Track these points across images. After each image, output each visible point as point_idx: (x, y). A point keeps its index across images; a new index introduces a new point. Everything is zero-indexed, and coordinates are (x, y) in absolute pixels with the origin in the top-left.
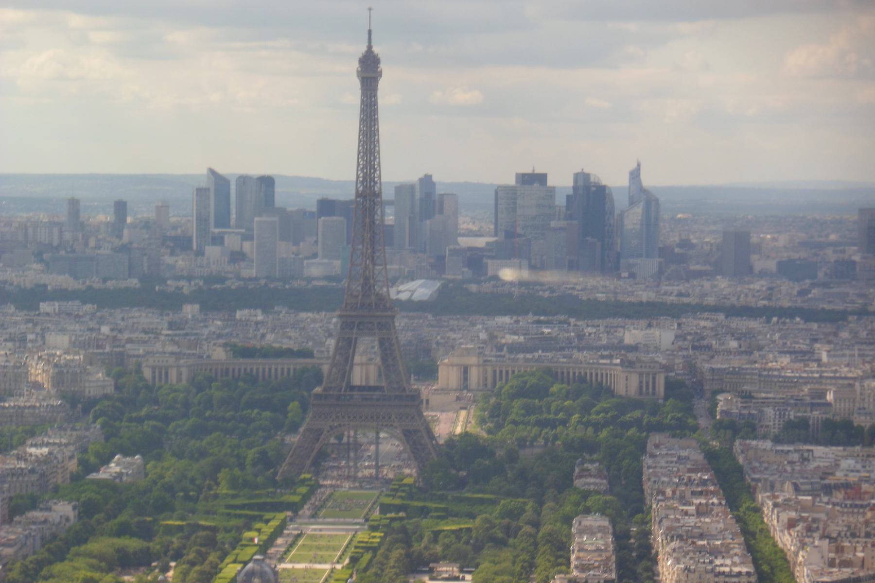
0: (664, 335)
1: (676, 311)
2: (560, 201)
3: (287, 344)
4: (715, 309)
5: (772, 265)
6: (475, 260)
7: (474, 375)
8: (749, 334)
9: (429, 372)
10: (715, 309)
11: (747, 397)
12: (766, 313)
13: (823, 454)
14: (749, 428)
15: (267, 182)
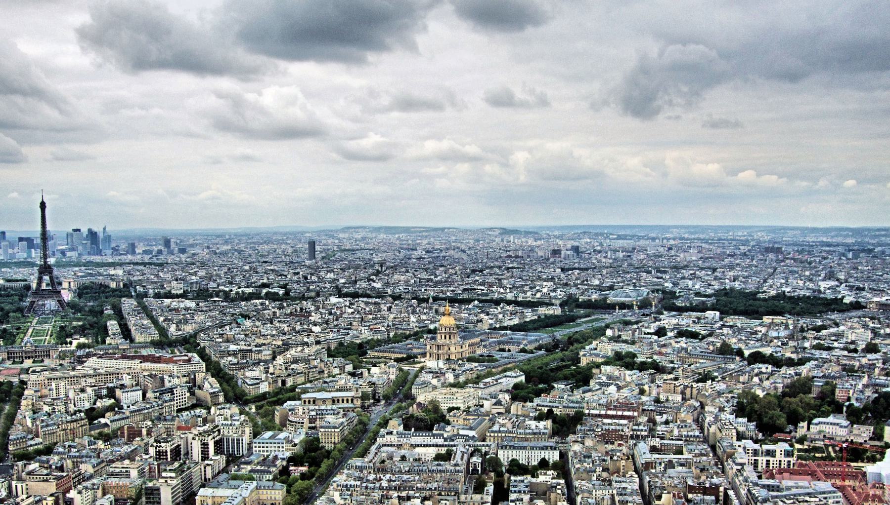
0: (119, 272)
1: (121, 265)
2: (85, 235)
3: (19, 278)
4: (129, 263)
5: (141, 251)
6: (63, 253)
7: (72, 284)
8: (142, 270)
9: (60, 284)
10: (129, 263)
11: (144, 287)
12: (144, 264)
13: (167, 301)
14: (146, 295)
15: (4, 233)
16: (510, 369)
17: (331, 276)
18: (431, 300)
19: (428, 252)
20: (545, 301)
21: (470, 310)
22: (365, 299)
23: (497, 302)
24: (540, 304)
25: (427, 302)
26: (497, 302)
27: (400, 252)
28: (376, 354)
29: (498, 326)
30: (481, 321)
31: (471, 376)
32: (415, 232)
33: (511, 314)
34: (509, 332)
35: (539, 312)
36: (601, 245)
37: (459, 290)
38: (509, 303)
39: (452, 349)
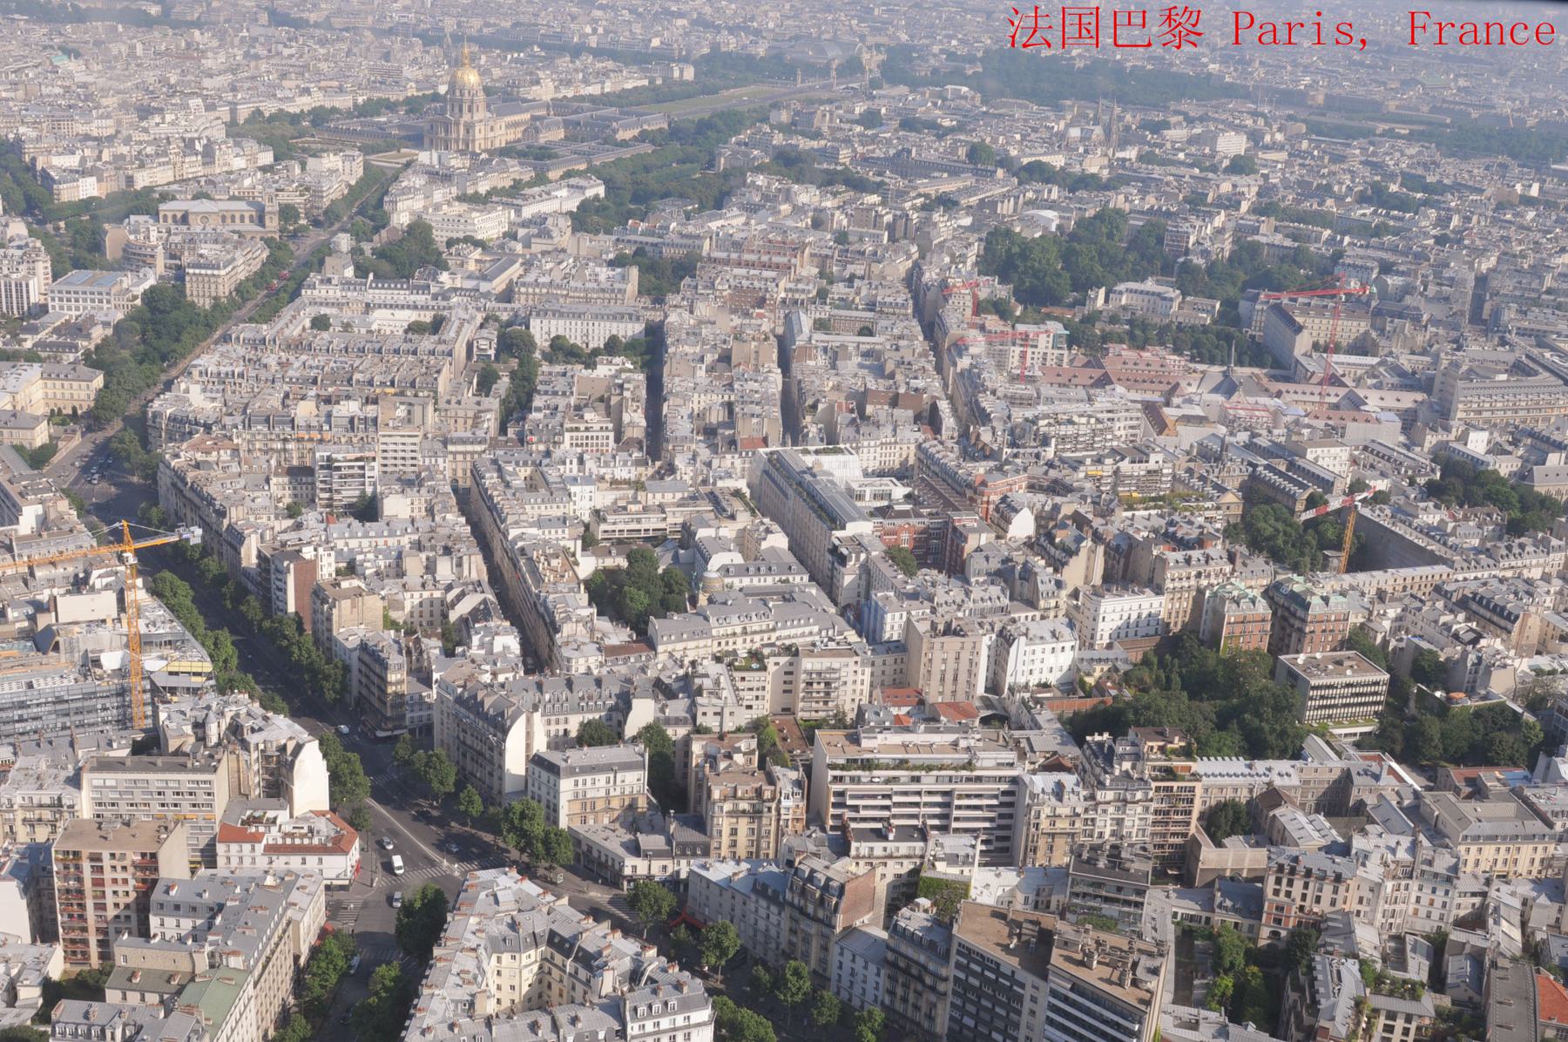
16: (579, 174)
31: (508, 183)
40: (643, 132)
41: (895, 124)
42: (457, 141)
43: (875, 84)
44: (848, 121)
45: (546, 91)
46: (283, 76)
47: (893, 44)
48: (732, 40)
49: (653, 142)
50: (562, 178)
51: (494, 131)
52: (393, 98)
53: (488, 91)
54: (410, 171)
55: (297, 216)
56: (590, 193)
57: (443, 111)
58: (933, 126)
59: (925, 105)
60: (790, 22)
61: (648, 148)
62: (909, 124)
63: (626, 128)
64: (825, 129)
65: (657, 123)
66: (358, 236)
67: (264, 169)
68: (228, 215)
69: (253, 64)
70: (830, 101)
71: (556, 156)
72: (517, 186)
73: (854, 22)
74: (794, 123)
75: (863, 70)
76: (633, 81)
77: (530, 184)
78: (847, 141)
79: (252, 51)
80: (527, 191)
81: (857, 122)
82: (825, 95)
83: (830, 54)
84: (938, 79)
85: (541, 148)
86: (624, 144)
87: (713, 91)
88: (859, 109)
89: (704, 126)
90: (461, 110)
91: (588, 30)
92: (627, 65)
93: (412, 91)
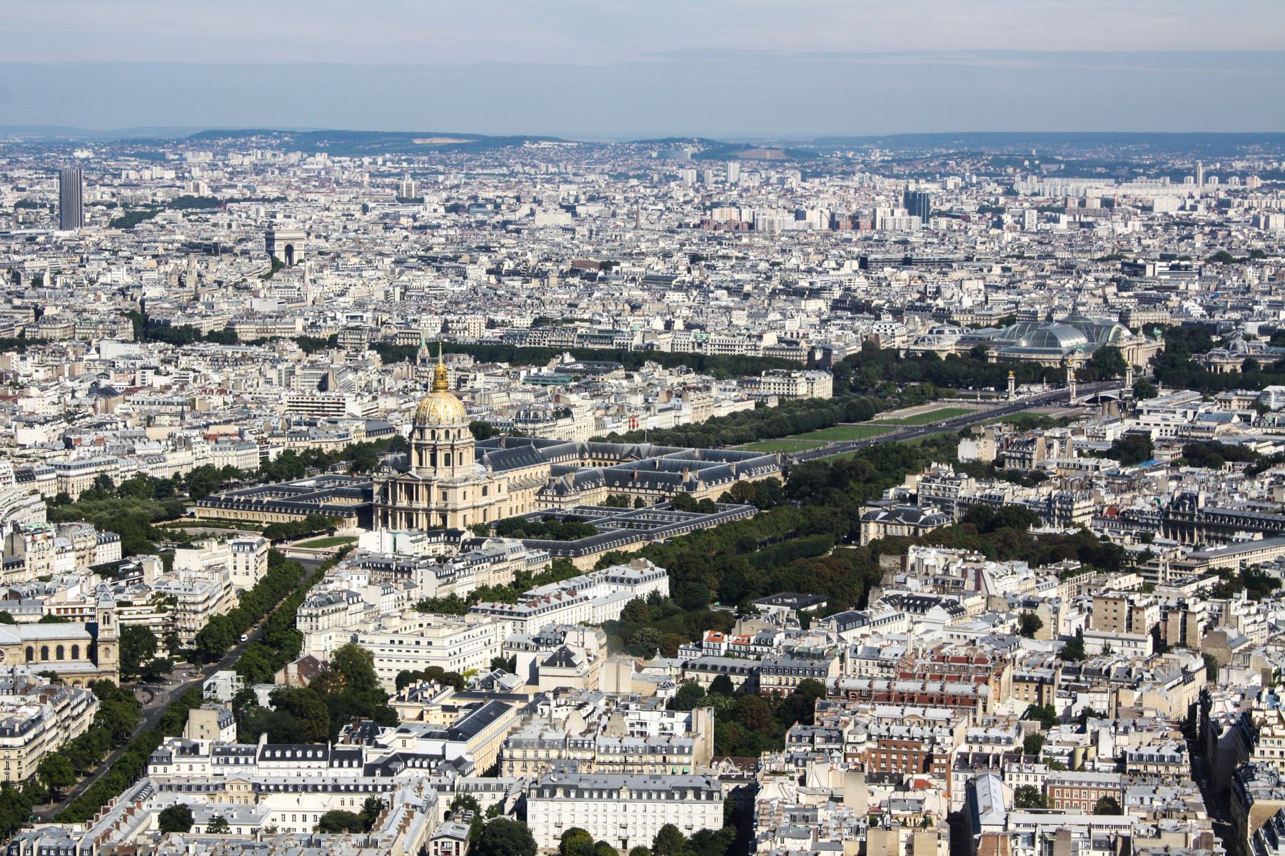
16: (626, 558)
17: (121, 276)
18: (424, 352)
19: (455, 209)
20: (790, 355)
21: (545, 382)
22: (214, 347)
23: (633, 360)
24: (771, 364)
25: (413, 359)
26: (633, 360)
27: (365, 209)
28: (214, 513)
29: (622, 430)
30: (567, 413)
32: (425, 150)
33: (669, 393)
34: (645, 446)
35: (763, 391)
36: (1011, 192)
37: (527, 321)
38: (671, 360)
39: (456, 498)
40: (741, 486)
41: (1177, 451)
42: (428, 512)
43: (1144, 390)
44: (1093, 453)
45: (583, 423)
46: (149, 421)
47: (1177, 322)
48: (900, 329)
49: (757, 503)
50: (599, 566)
51: (483, 493)
52: (328, 448)
53: (481, 431)
54: (343, 565)
55: (154, 648)
56: (643, 591)
57: (404, 466)
58: (1238, 453)
59: (1227, 419)
60: (1002, 296)
61: (747, 513)
62: (1202, 453)
63: (710, 478)
64: (1052, 467)
65: (766, 468)
66: (252, 673)
67: (106, 571)
68: (37, 648)
69: (101, 403)
70: (1064, 422)
71: (591, 531)
72: (522, 582)
73: (1112, 289)
74: (1000, 461)
75: (1121, 367)
76: (727, 401)
77: (543, 580)
78: (1088, 486)
79: (104, 383)
80: (538, 591)
81: (1109, 454)
82: (1055, 413)
83: (1065, 344)
84: (1252, 377)
85: (568, 518)
86: (707, 506)
87: (865, 414)
88: (1114, 432)
89: (839, 476)
90: (434, 463)
91: (658, 324)
92: (719, 378)
93: (358, 436)
